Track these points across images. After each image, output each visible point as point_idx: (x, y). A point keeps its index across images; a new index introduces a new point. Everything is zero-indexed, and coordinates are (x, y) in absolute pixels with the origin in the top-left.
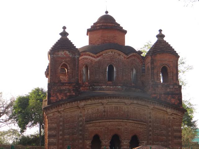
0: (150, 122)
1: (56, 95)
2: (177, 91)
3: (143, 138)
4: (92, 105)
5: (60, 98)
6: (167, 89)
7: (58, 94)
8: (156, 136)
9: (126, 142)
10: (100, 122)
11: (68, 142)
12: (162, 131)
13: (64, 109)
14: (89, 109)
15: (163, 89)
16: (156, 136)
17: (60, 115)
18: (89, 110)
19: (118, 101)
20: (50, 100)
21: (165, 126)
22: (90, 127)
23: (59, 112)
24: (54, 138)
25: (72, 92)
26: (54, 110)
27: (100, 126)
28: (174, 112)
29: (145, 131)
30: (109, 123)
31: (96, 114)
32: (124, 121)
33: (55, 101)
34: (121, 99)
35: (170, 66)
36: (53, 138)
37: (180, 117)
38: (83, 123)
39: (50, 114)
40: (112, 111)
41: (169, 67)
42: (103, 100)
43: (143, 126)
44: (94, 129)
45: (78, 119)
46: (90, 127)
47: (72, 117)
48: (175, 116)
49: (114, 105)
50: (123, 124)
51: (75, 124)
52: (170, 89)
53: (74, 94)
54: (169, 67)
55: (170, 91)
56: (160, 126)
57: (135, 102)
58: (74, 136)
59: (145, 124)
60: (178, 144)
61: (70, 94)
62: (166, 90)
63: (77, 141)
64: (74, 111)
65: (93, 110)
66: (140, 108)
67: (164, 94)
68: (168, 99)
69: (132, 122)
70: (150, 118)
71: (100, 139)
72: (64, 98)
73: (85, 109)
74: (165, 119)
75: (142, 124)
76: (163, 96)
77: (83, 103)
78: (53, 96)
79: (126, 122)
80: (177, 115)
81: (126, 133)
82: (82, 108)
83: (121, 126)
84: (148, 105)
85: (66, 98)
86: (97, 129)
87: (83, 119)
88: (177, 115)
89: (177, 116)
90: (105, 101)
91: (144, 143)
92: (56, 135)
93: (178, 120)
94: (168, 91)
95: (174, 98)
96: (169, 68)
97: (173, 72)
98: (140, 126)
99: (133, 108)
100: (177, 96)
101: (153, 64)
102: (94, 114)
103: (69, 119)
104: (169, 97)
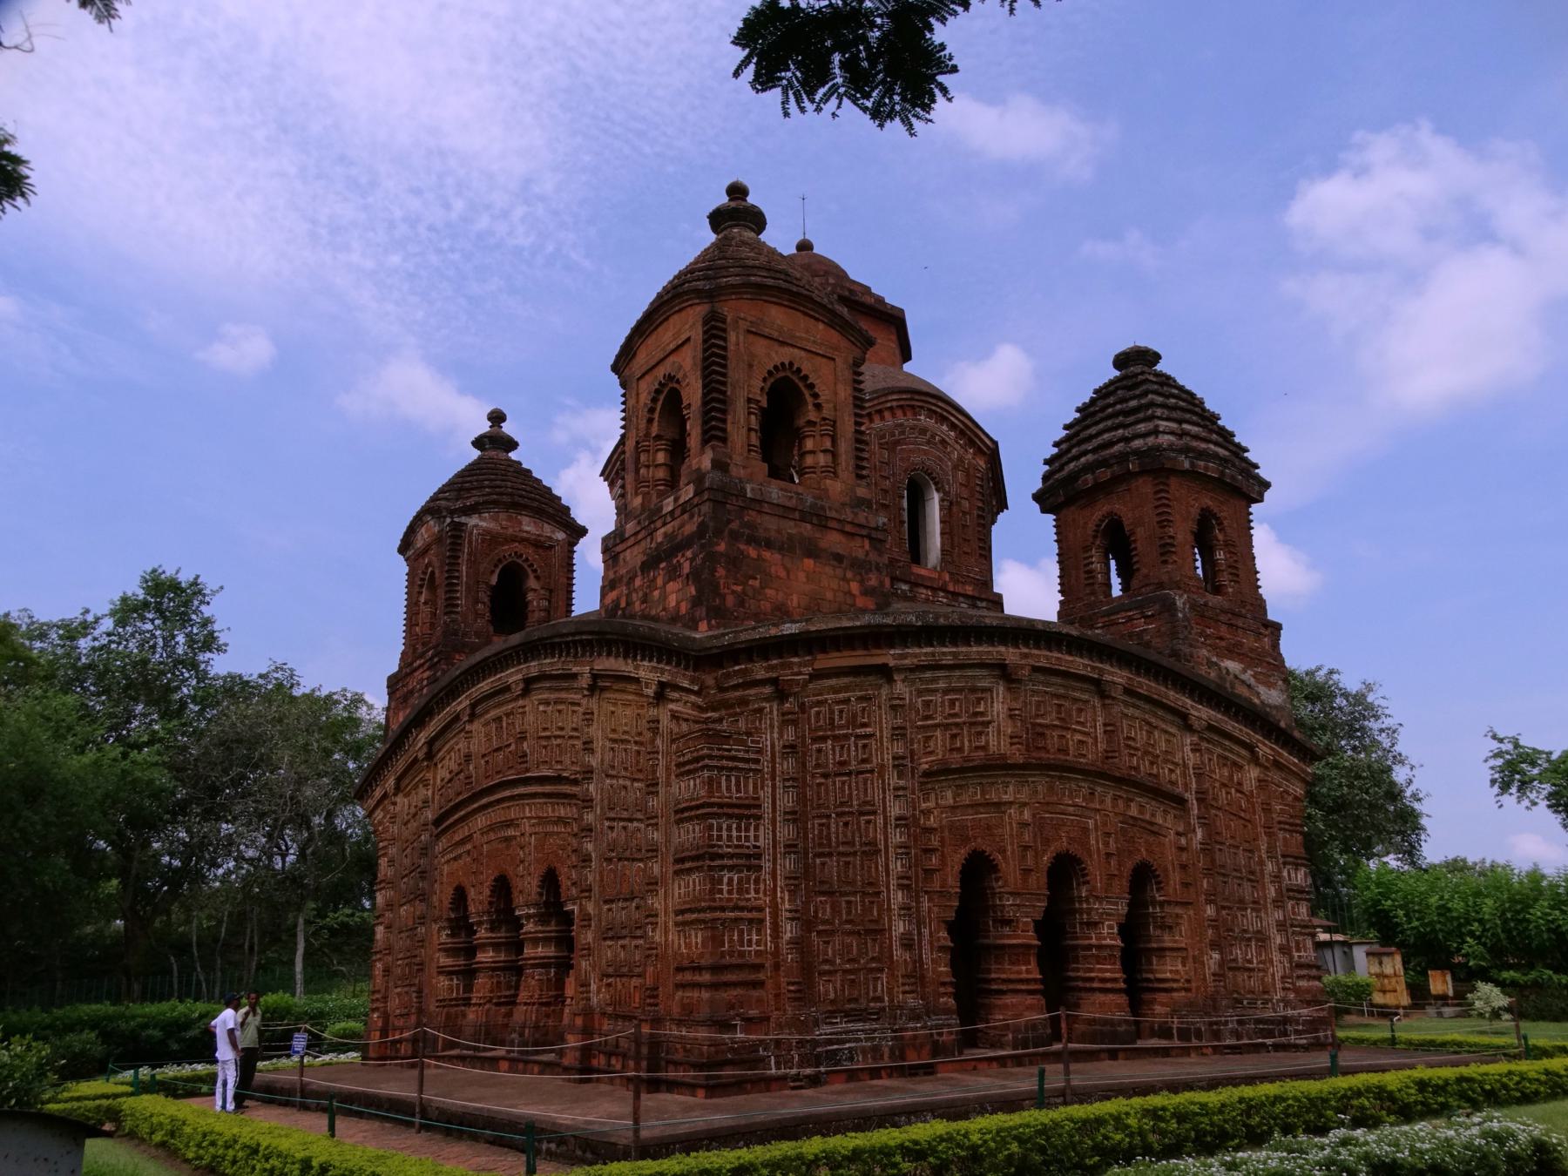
2: (692, 516)
6: (656, 530)
10: (462, 819)
12: (630, 820)
15: (640, 536)
16: (609, 860)
26: (378, 793)
28: (663, 672)
30: (481, 821)
32: (516, 791)
35: (679, 376)
37: (693, 698)
44: (455, 859)
52: (664, 524)
54: (678, 382)
55: (665, 535)
57: (533, 668)
60: (691, 911)
66: (563, 695)
68: (656, 593)
75: (566, 796)
77: (423, 737)
83: (510, 824)
84: (575, 670)
90: (462, 703)
100: (689, 554)
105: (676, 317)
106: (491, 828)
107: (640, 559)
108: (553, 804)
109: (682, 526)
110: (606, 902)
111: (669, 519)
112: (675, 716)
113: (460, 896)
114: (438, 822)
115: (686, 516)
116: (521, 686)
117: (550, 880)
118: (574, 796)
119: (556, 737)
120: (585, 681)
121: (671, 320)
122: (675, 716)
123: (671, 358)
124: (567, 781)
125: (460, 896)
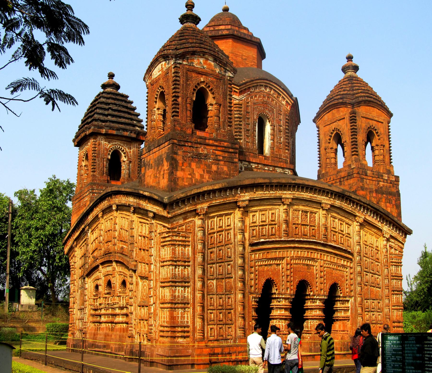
0: (359, 253)
1: (190, 165)
2: (393, 186)
3: (347, 290)
4: (262, 203)
5: (197, 176)
6: (380, 181)
7: (194, 165)
8: (367, 285)
9: (320, 300)
10: (277, 248)
11: (215, 296)
12: (375, 274)
13: (209, 207)
14: (256, 211)
15: (373, 179)
16: (367, 285)
17: (198, 222)
18: (257, 214)
19: (311, 196)
20: (178, 179)
21: (379, 264)
22: (259, 260)
23: (198, 214)
24: (185, 287)
25: (222, 163)
27: (275, 259)
29: (351, 274)
30: (292, 253)
31: (270, 227)
33: (187, 184)
34: (314, 193)
36: (182, 287)
37: (400, 244)
38: (244, 248)
39: (178, 218)
40: (297, 222)
41: (377, 133)
42: (285, 192)
43: (348, 262)
44: (266, 265)
45: (235, 235)
46: (259, 260)
47: (222, 231)
48: (392, 243)
49: (301, 207)
50: (316, 255)
51: (229, 250)
53: (225, 169)
56: (372, 263)
58: (227, 280)
59: (350, 256)
60: (398, 306)
61: (218, 168)
62: (378, 184)
63: (232, 296)
64: (226, 215)
65: (264, 214)
67: (377, 191)
69: (332, 252)
70: (359, 243)
71: (274, 291)
72: (206, 176)
73: (247, 212)
74: (379, 249)
76: (374, 195)
78: (183, 170)
79: (321, 250)
80: (396, 239)
81: (321, 277)
82: (244, 207)
83: (313, 259)
84: (357, 214)
85: (209, 178)
86: (270, 265)
87: (245, 239)
88: (396, 239)
89: (397, 242)
91: (348, 303)
92: (188, 278)
93: (397, 252)
94: (381, 186)
95: (389, 203)
96: (378, 136)
97: (384, 146)
98: (342, 262)
99: (332, 218)
101: (356, 123)
102: (266, 225)
103: (215, 234)
104: (384, 200)
105: (377, 110)
106: (299, 258)
107: (374, 188)
108: (338, 259)
109: (390, 187)
110: (366, 299)
111: (385, 181)
112: (391, 247)
113: (269, 284)
114: (252, 245)
115: (391, 185)
116: (329, 206)
117: (334, 288)
118: (351, 259)
119: (339, 233)
120: (361, 220)
121: (375, 109)
122: (391, 247)
123: (375, 122)
124: (349, 253)
125: (269, 284)
